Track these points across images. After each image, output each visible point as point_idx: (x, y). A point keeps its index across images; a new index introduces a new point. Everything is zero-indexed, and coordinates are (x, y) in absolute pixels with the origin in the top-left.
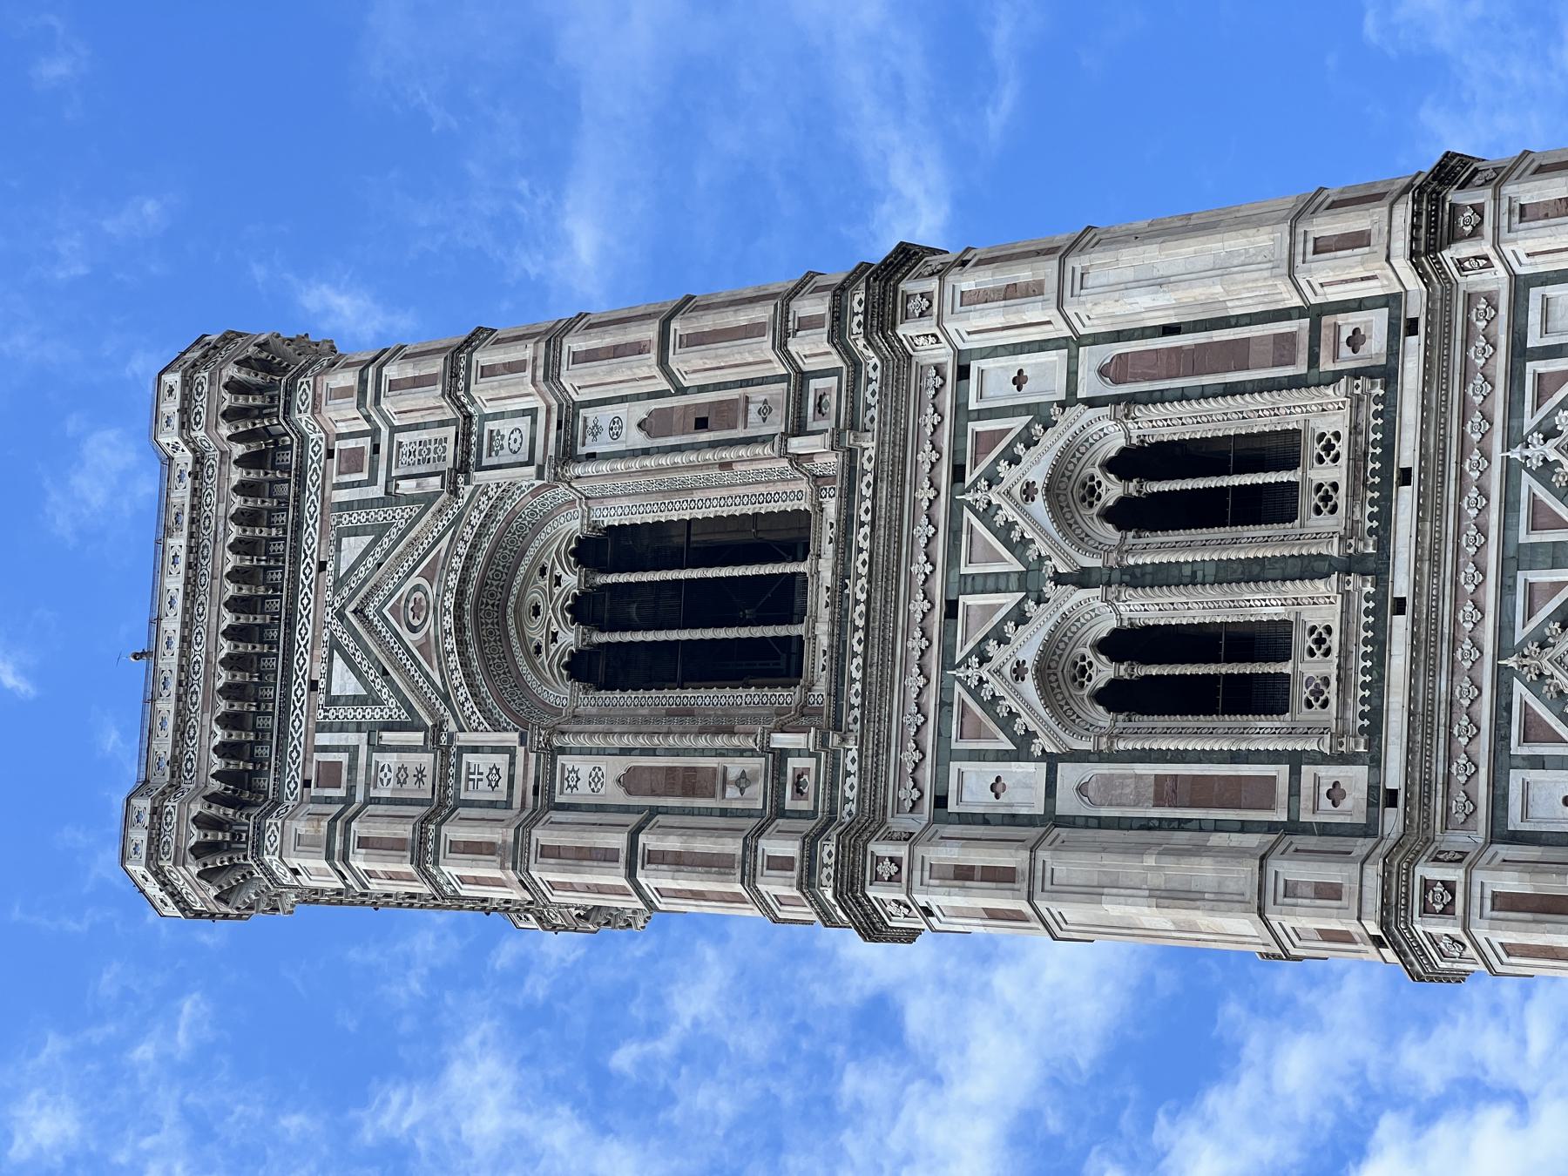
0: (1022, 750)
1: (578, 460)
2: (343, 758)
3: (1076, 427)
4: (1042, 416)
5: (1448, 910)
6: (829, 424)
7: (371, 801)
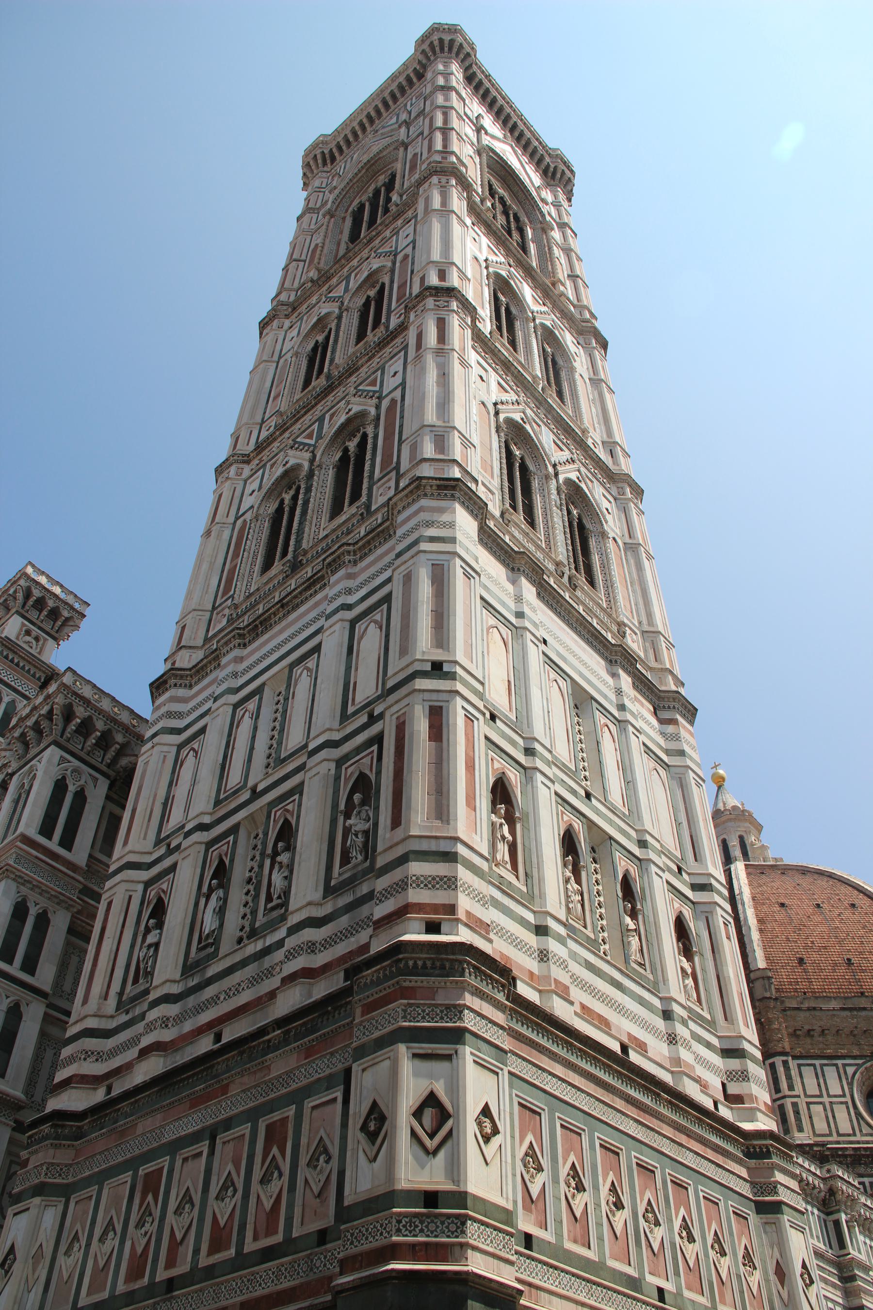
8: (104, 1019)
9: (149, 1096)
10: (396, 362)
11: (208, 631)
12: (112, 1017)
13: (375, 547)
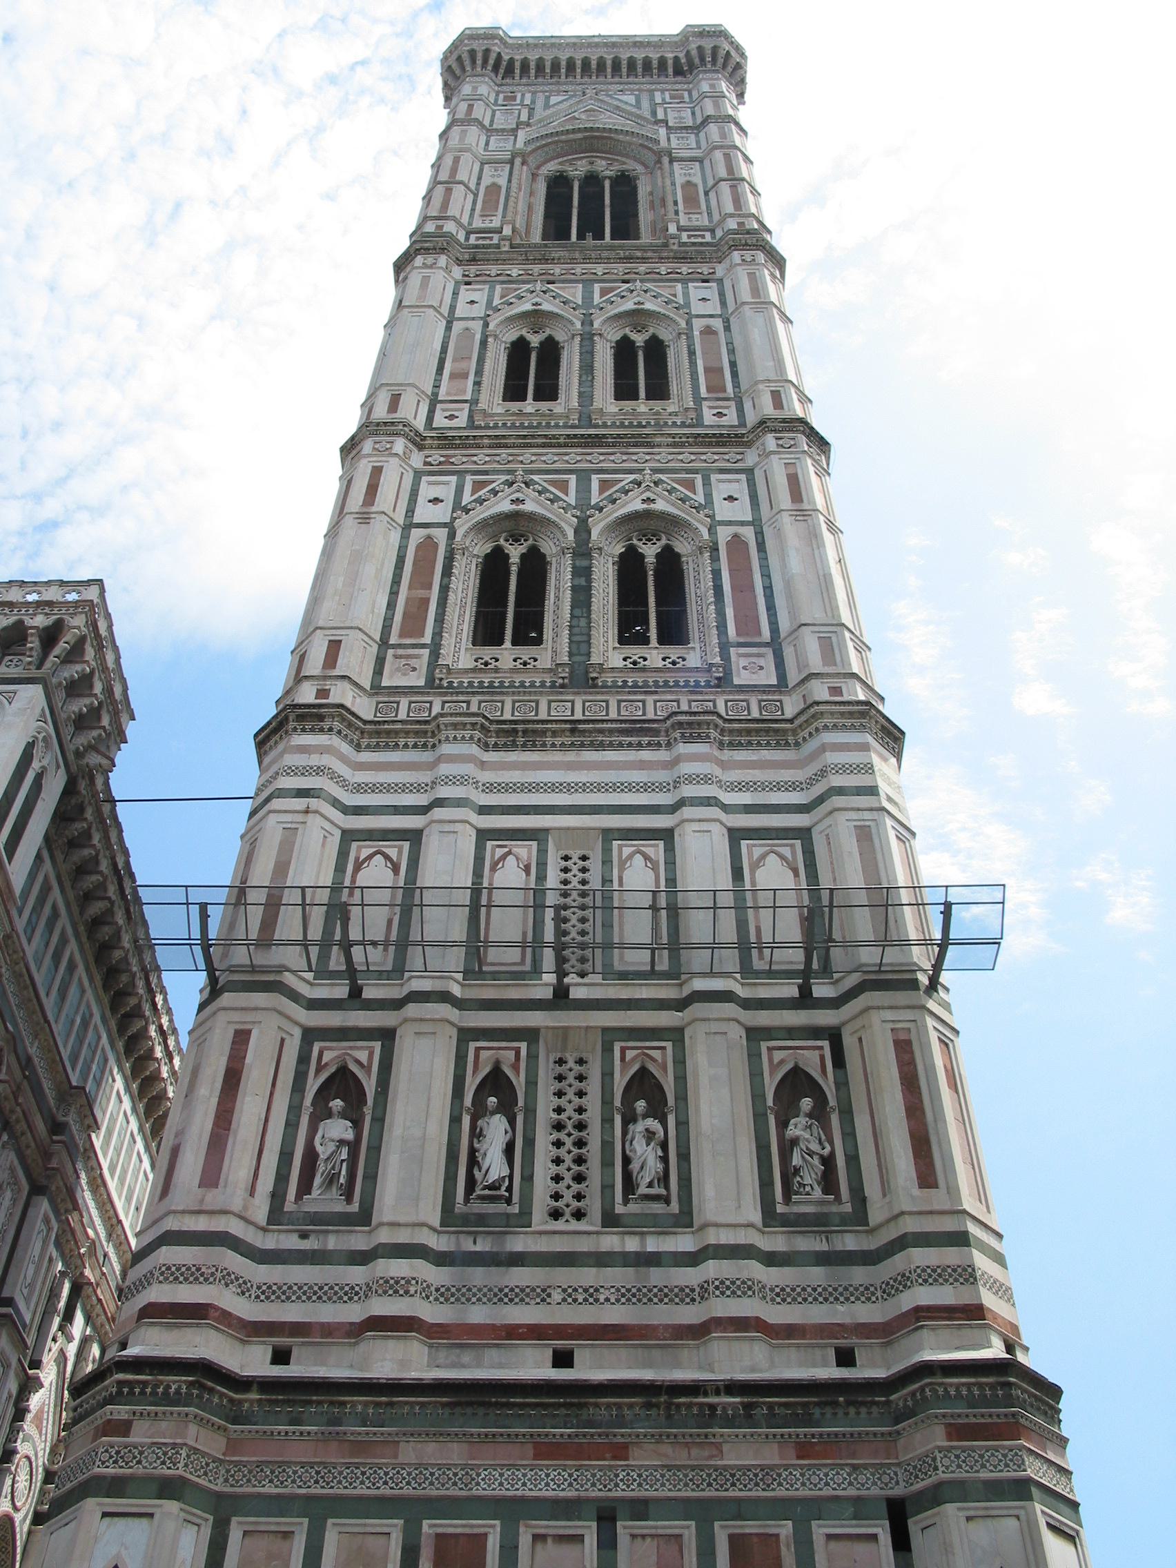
1: (671, 162)
7: (494, 112)
8: (251, 1228)
9: (422, 1405)
10: (730, 481)
11: (378, 671)
12: (264, 1230)
13: (759, 744)
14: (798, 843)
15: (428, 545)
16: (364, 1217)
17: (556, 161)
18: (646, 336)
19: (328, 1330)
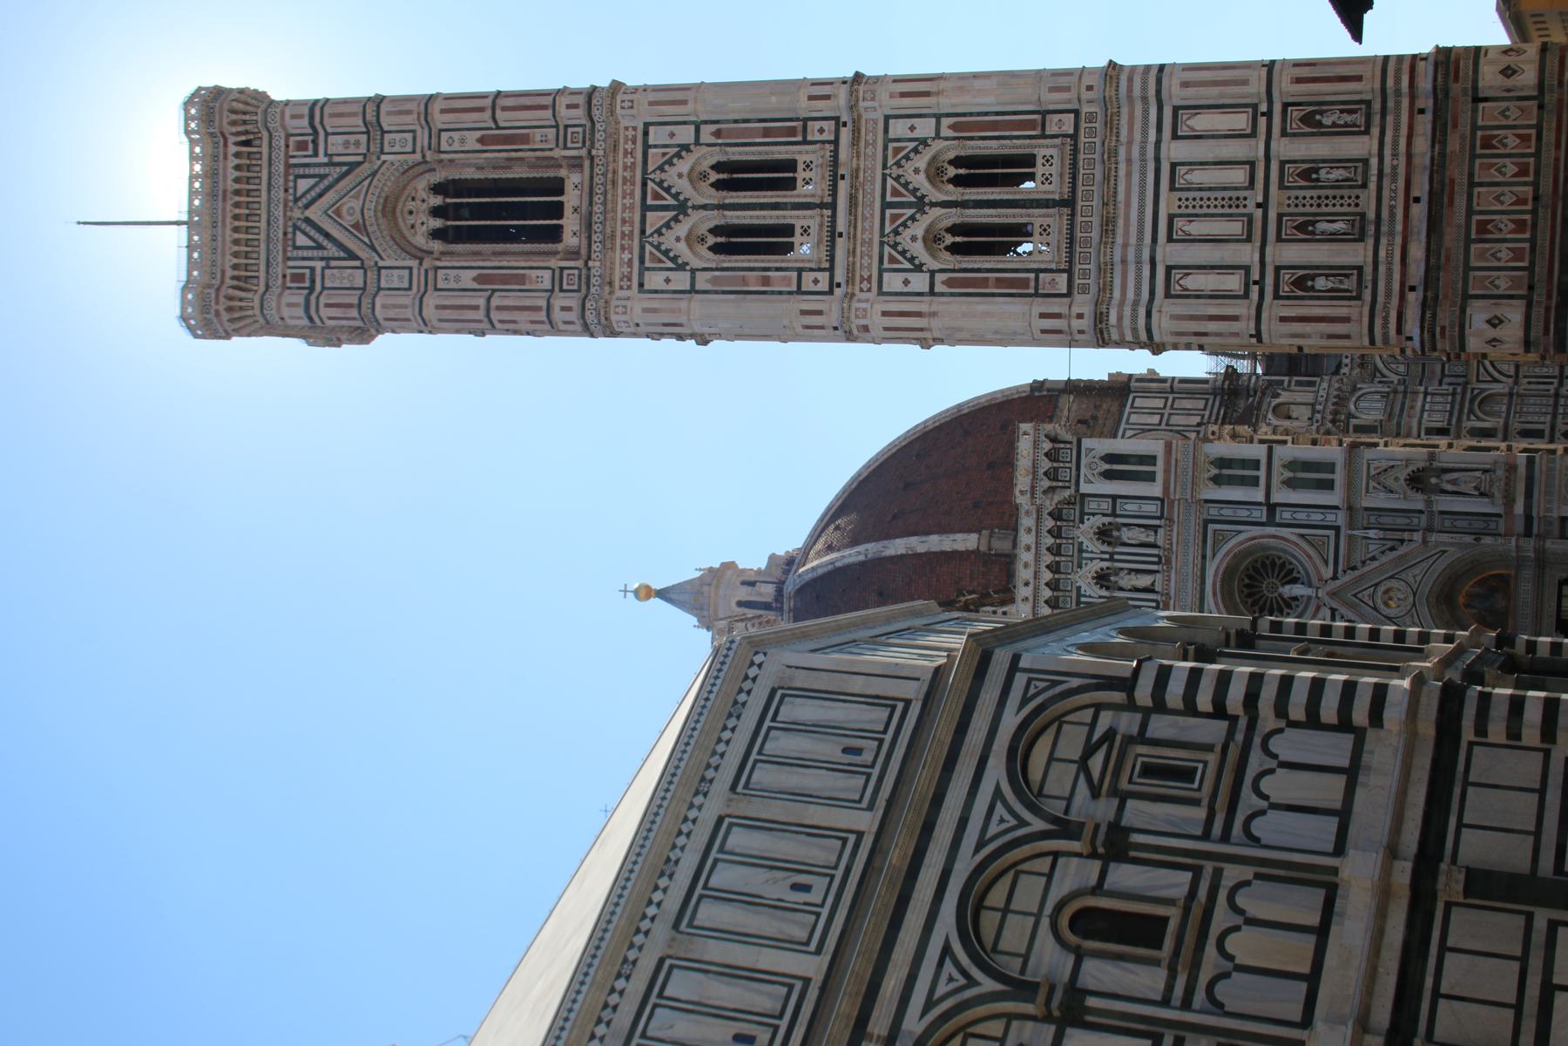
0: (681, 267)
1: (443, 152)
2: (307, 271)
3: (702, 153)
4: (685, 148)
5: (865, 317)
6: (580, 145)
14: (1180, 112)
15: (949, 283)
16: (1360, 269)
17: (410, 239)
18: (710, 171)
19: (1403, 275)
